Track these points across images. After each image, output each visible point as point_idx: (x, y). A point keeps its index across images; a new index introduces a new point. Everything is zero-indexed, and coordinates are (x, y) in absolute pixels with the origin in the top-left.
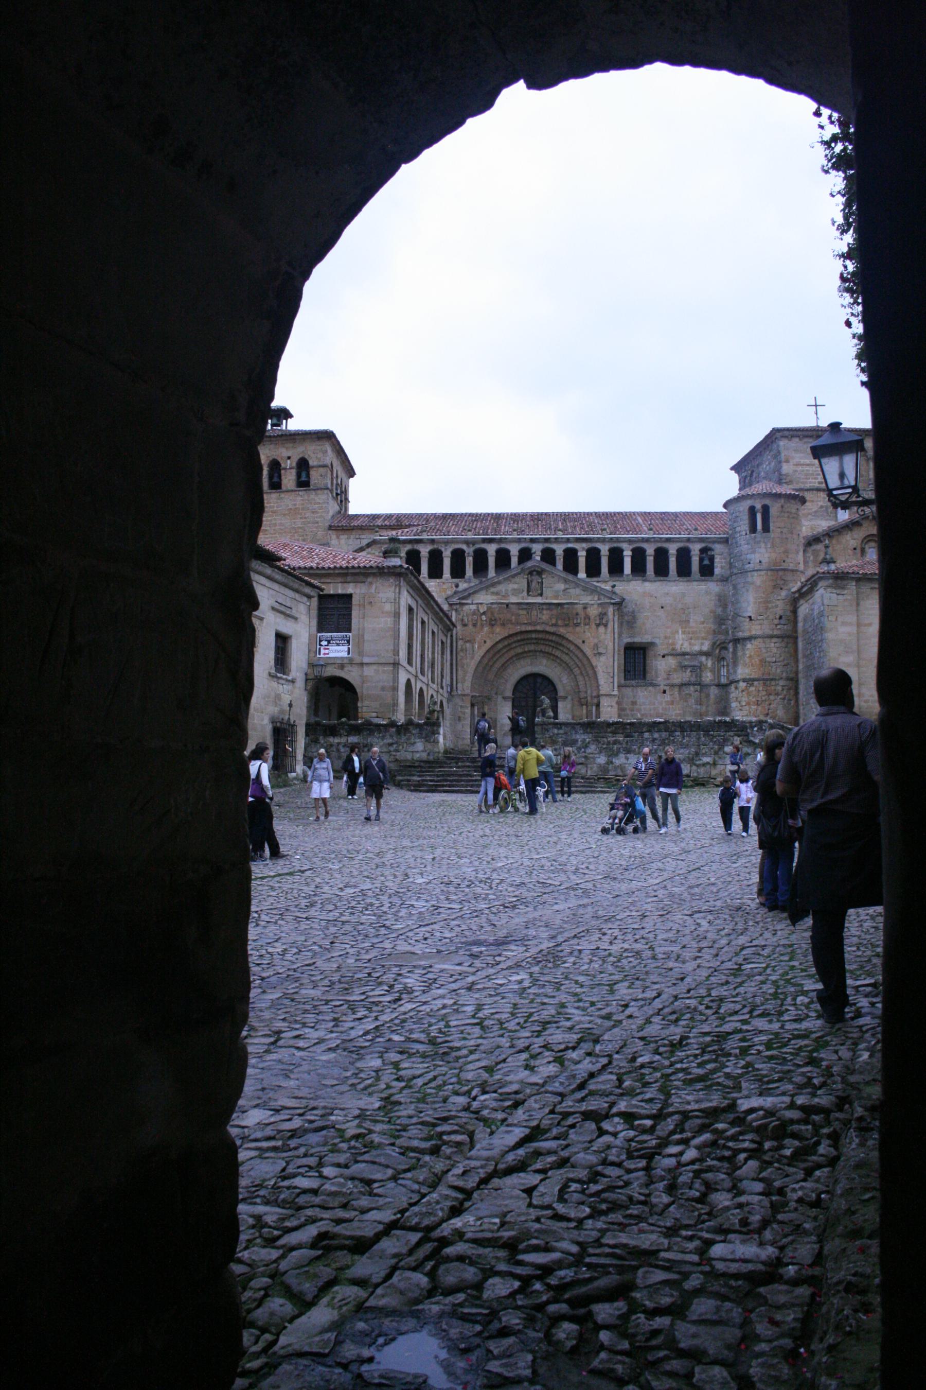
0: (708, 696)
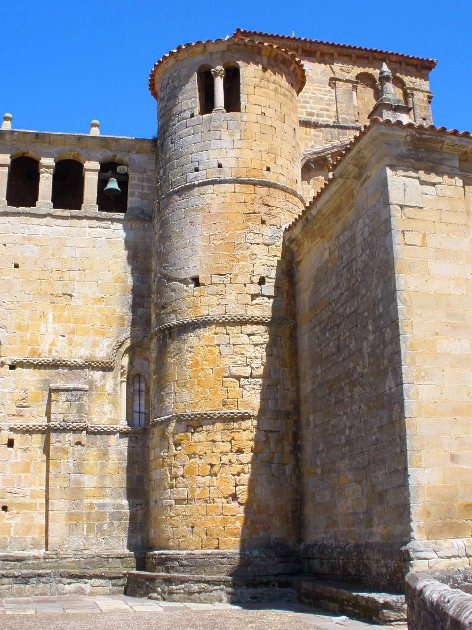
0: (104, 454)
